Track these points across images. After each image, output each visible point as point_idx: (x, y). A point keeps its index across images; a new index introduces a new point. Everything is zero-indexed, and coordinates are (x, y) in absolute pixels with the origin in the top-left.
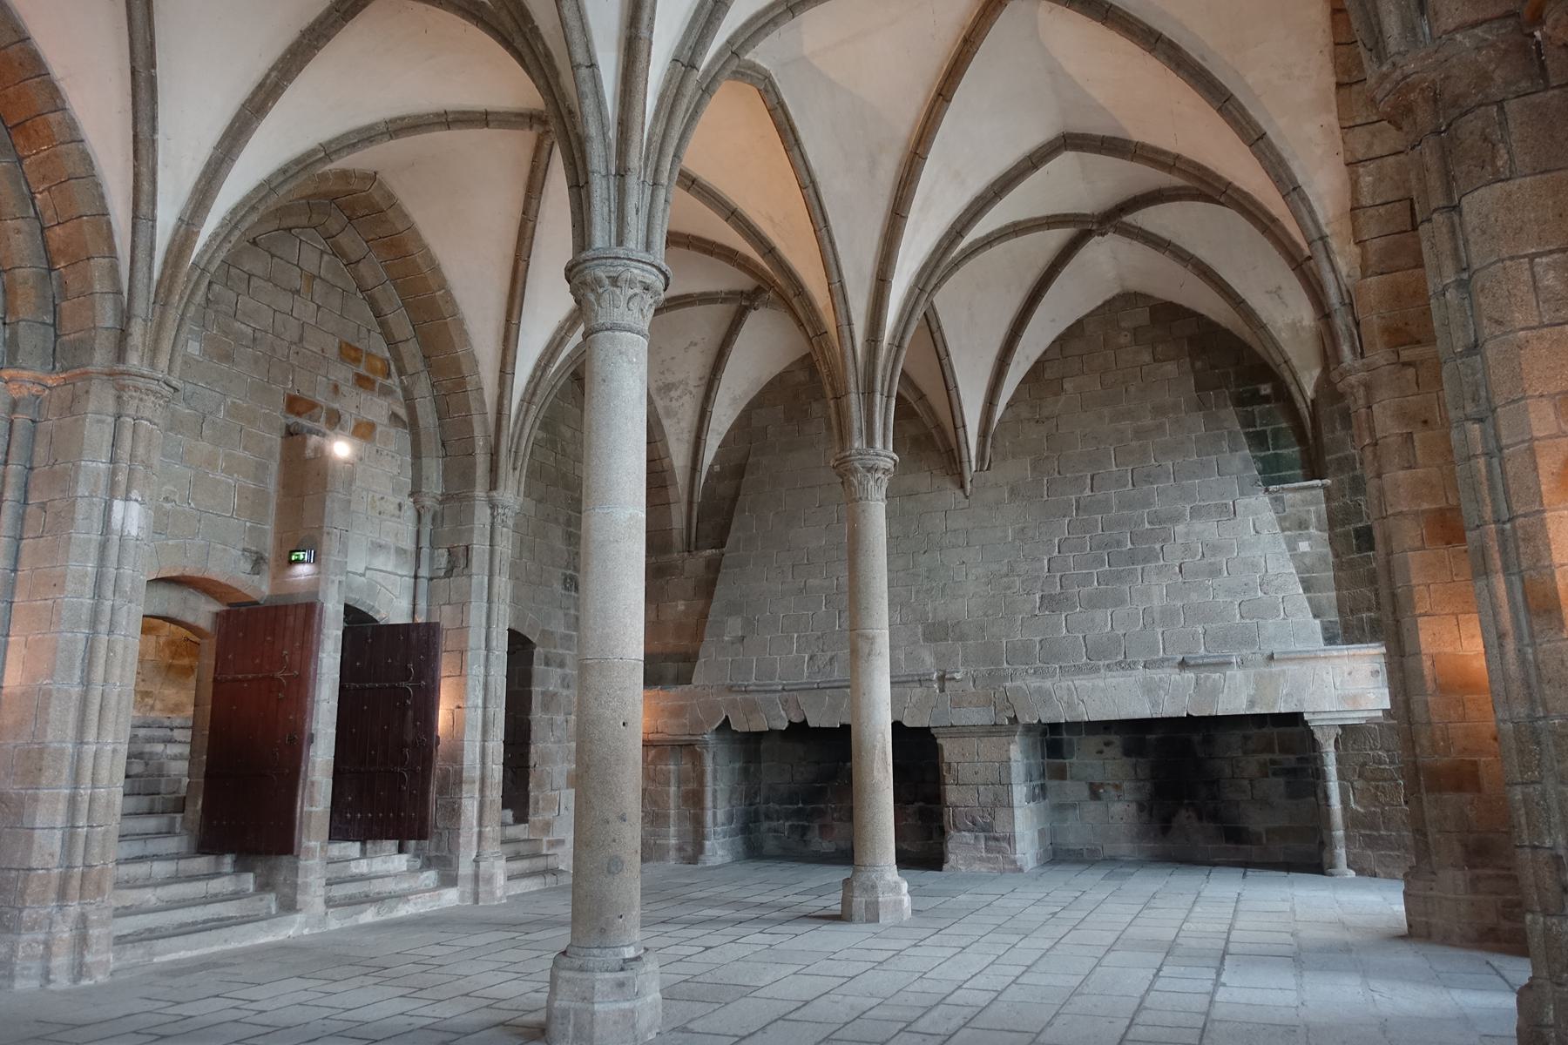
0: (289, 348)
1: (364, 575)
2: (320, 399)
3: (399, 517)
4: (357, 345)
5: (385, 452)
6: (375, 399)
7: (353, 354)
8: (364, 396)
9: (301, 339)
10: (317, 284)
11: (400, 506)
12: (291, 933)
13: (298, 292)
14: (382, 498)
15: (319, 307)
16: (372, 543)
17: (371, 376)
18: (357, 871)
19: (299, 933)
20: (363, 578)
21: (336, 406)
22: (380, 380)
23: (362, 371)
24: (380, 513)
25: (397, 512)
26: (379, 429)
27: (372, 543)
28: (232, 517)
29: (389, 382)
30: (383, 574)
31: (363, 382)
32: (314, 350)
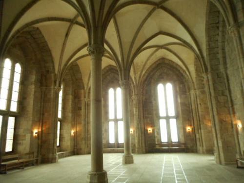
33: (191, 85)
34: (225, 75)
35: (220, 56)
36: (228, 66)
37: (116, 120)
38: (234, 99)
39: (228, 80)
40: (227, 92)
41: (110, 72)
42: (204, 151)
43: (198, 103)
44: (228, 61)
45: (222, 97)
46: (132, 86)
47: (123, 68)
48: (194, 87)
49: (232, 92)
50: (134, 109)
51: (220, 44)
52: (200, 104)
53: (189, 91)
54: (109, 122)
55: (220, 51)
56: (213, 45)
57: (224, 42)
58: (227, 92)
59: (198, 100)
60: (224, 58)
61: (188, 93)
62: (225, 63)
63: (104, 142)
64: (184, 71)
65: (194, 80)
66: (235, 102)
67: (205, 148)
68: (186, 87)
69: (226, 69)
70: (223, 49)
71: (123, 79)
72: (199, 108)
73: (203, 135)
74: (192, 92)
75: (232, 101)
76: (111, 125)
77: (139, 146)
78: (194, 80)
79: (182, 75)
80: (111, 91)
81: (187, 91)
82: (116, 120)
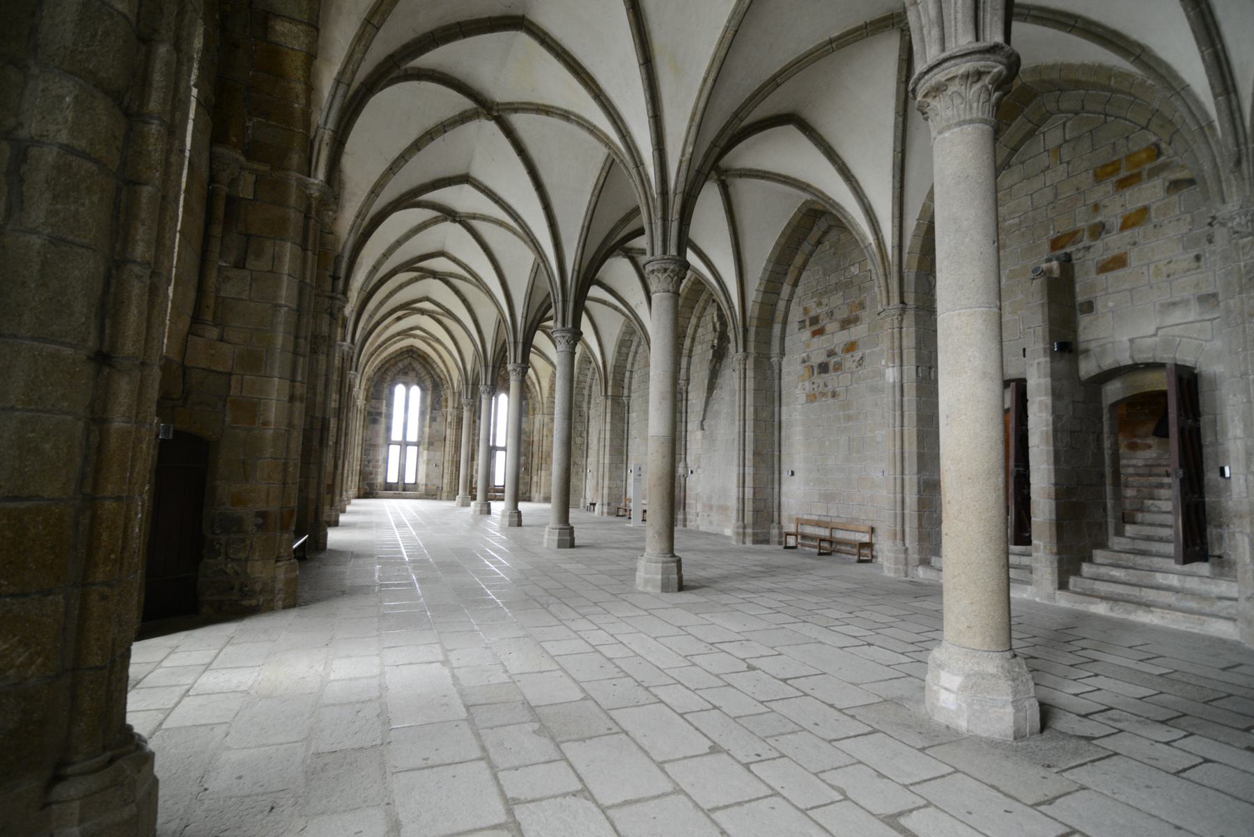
0: (1046, 209)
1: (1155, 335)
2: (1081, 224)
3: (1199, 267)
4: (1115, 158)
5: (1166, 222)
6: (1144, 186)
7: (1109, 169)
8: (1128, 193)
9: (1056, 195)
10: (1065, 151)
11: (1198, 258)
12: (1025, 596)
13: (1048, 168)
14: (1170, 262)
15: (1068, 163)
16: (1162, 305)
17: (1135, 171)
18: (1165, 582)
19: (1031, 598)
20: (1154, 338)
21: (1099, 219)
22: (1147, 166)
23: (1123, 173)
24: (1168, 276)
25: (1194, 265)
26: (1153, 207)
27: (1162, 305)
28: (1020, 338)
29: (1162, 159)
30: (1182, 326)
31: (1123, 184)
32: (1069, 194)
33: (537, 405)
34: (586, 415)
35: (586, 392)
36: (592, 406)
37: (404, 444)
38: (590, 442)
39: (588, 422)
40: (585, 432)
41: (406, 356)
42: (541, 499)
43: (545, 434)
44: (592, 401)
45: (579, 438)
46: (449, 392)
47: (470, 382)
48: (543, 411)
49: (590, 435)
50: (448, 431)
51: (588, 380)
52: (547, 436)
53: (534, 414)
54: (389, 445)
55: (587, 388)
56: (581, 378)
57: (593, 379)
58: (585, 434)
59: (545, 430)
60: (590, 396)
61: (531, 417)
62: (589, 402)
63: (380, 480)
64: (533, 384)
65: (545, 400)
66: (590, 446)
67: (542, 495)
68: (531, 406)
69: (589, 408)
70: (591, 387)
71: (469, 397)
72: (544, 442)
73: (543, 478)
74: (538, 418)
75: (588, 444)
76: (394, 451)
77: (451, 488)
78: (545, 400)
79: (528, 387)
80: (400, 390)
81: (531, 412)
82: (404, 444)
